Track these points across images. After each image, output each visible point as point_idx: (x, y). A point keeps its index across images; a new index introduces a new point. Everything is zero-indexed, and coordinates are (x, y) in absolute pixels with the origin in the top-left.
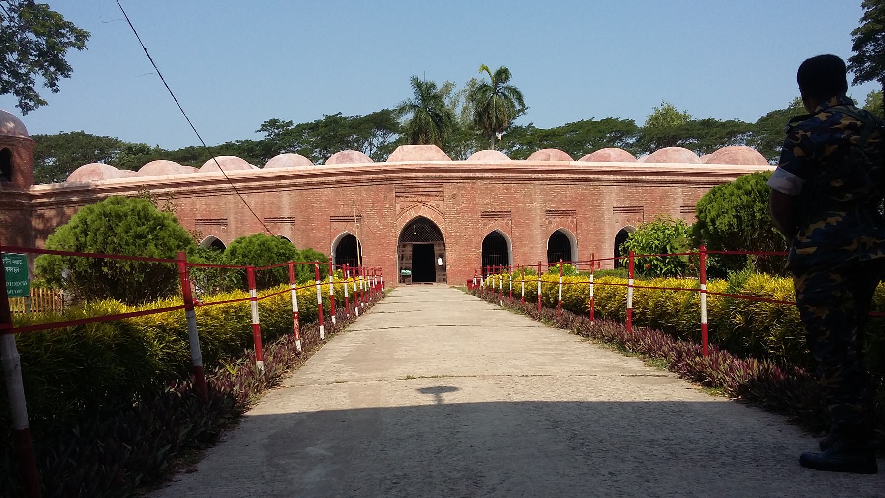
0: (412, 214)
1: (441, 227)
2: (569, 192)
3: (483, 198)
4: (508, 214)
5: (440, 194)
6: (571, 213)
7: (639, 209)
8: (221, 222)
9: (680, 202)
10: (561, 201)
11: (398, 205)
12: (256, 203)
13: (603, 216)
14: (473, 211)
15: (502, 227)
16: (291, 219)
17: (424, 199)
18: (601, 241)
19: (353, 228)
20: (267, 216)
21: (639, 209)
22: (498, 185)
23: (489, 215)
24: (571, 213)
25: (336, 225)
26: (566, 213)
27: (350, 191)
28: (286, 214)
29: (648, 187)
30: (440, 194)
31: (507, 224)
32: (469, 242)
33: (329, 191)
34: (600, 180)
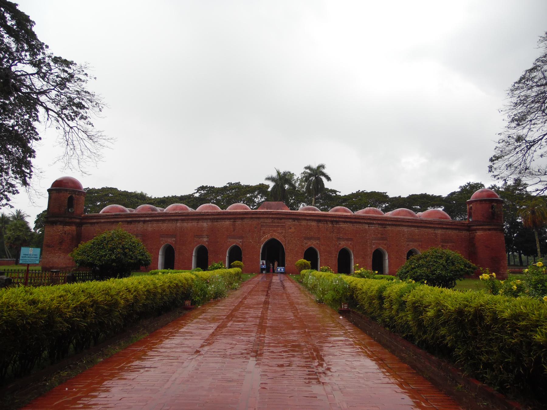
1: (283, 244)
5: (283, 227)
11: (262, 232)
13: (367, 242)
17: (275, 229)
19: (238, 242)
22: (314, 224)
24: (351, 240)
26: (347, 240)
31: (317, 244)
33: (227, 223)
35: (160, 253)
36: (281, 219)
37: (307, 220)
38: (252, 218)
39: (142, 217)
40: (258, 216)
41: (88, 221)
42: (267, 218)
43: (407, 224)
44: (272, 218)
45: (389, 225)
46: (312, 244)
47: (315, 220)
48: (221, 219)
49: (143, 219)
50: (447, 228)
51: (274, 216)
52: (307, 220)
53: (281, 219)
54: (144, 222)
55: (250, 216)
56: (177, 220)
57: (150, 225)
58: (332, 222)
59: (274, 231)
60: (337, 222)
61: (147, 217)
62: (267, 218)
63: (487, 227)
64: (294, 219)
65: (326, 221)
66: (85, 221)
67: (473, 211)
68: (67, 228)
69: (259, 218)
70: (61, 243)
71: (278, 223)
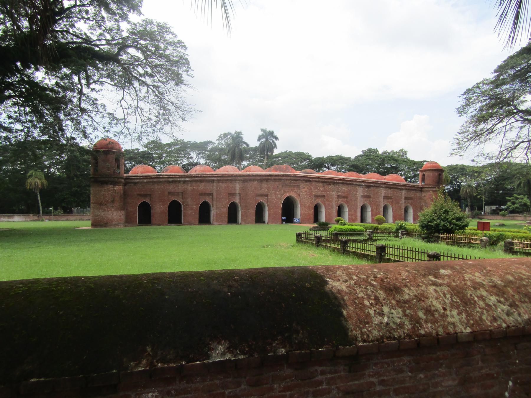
0: (287, 195)
2: (344, 188)
4: (324, 196)
6: (346, 197)
7: (369, 197)
8: (211, 194)
9: (383, 195)
10: (343, 192)
12: (225, 187)
14: (311, 194)
15: (321, 201)
16: (240, 194)
18: (357, 209)
20: (230, 192)
21: (369, 197)
22: (320, 184)
23: (317, 196)
25: (258, 198)
27: (264, 185)
28: (238, 192)
29: (372, 188)
30: (299, 187)
32: (309, 207)
33: (255, 183)
34: (356, 185)
37: (316, 181)
38: (275, 179)
39: (182, 177)
40: (280, 178)
41: (131, 181)
42: (287, 180)
43: (383, 186)
44: (290, 180)
45: (372, 186)
46: (319, 201)
47: (322, 182)
48: (250, 180)
49: (182, 179)
50: (409, 189)
51: (292, 178)
52: (316, 181)
53: (297, 180)
54: (185, 182)
55: (273, 178)
56: (213, 181)
57: (190, 185)
58: (334, 184)
59: (292, 190)
60: (337, 184)
61: (187, 177)
62: (287, 180)
64: (306, 181)
65: (330, 183)
66: (127, 181)
69: (280, 180)
70: (113, 201)
71: (295, 183)
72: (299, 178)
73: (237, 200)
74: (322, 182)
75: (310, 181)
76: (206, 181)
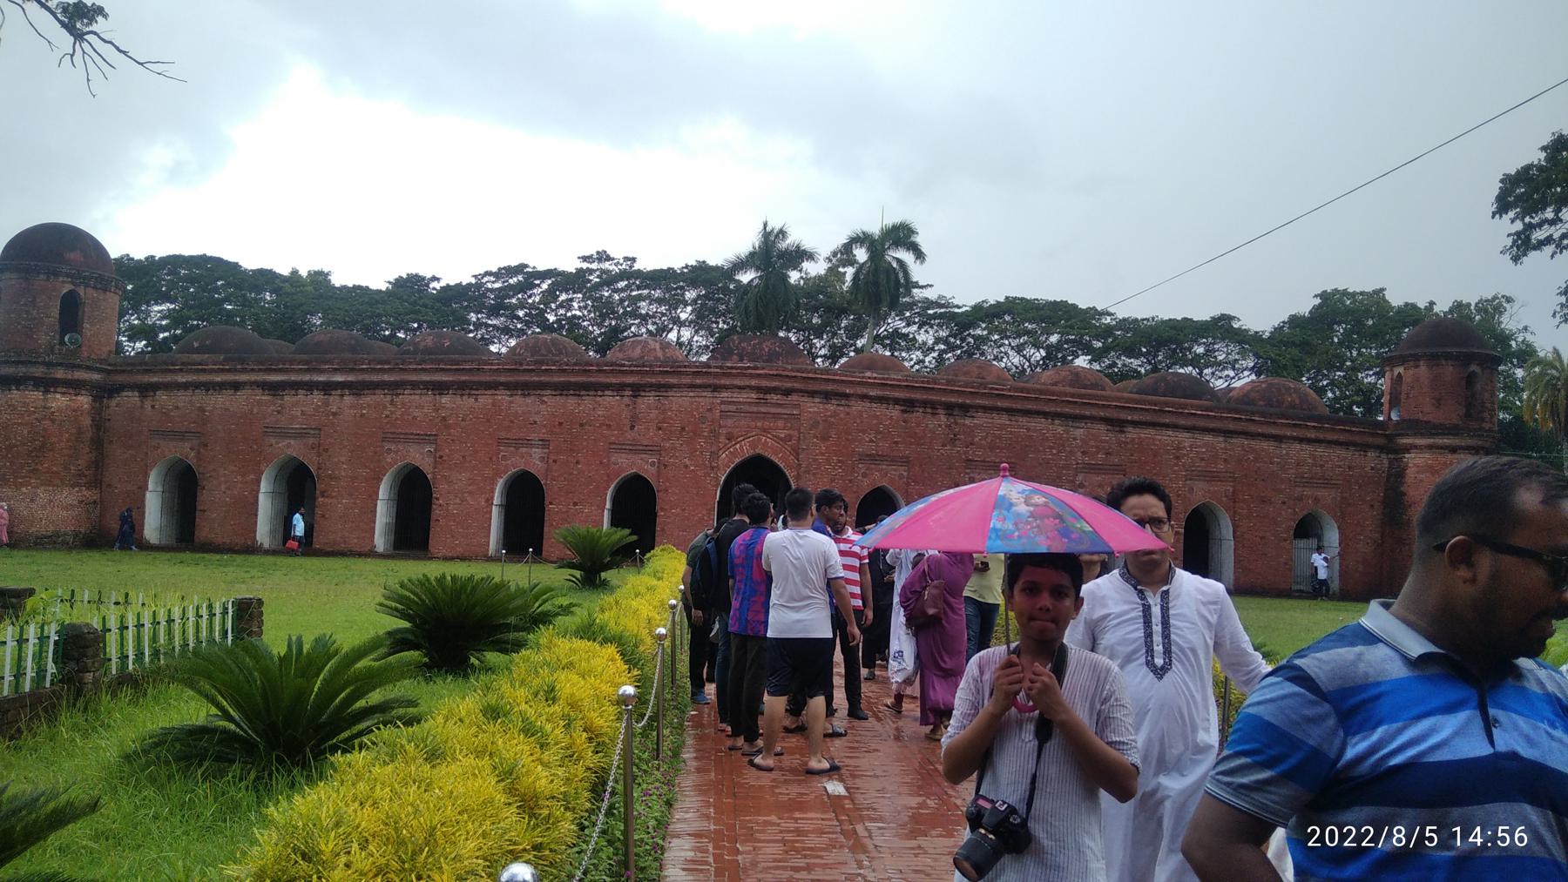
0: (744, 450)
3: (864, 432)
35: (384, 491)
36: (787, 392)
37: (872, 399)
47: (897, 401)
49: (322, 378)
54: (327, 388)
63: (1446, 441)
64: (827, 396)
67: (1404, 388)
68: (59, 401)
72: (797, 385)
73: (534, 461)
74: (897, 401)
75: (847, 396)
76: (414, 385)
